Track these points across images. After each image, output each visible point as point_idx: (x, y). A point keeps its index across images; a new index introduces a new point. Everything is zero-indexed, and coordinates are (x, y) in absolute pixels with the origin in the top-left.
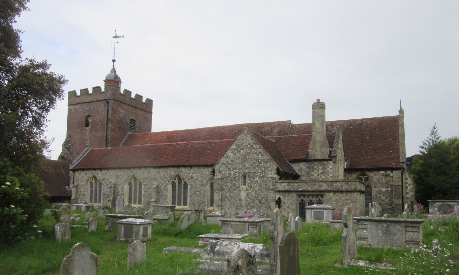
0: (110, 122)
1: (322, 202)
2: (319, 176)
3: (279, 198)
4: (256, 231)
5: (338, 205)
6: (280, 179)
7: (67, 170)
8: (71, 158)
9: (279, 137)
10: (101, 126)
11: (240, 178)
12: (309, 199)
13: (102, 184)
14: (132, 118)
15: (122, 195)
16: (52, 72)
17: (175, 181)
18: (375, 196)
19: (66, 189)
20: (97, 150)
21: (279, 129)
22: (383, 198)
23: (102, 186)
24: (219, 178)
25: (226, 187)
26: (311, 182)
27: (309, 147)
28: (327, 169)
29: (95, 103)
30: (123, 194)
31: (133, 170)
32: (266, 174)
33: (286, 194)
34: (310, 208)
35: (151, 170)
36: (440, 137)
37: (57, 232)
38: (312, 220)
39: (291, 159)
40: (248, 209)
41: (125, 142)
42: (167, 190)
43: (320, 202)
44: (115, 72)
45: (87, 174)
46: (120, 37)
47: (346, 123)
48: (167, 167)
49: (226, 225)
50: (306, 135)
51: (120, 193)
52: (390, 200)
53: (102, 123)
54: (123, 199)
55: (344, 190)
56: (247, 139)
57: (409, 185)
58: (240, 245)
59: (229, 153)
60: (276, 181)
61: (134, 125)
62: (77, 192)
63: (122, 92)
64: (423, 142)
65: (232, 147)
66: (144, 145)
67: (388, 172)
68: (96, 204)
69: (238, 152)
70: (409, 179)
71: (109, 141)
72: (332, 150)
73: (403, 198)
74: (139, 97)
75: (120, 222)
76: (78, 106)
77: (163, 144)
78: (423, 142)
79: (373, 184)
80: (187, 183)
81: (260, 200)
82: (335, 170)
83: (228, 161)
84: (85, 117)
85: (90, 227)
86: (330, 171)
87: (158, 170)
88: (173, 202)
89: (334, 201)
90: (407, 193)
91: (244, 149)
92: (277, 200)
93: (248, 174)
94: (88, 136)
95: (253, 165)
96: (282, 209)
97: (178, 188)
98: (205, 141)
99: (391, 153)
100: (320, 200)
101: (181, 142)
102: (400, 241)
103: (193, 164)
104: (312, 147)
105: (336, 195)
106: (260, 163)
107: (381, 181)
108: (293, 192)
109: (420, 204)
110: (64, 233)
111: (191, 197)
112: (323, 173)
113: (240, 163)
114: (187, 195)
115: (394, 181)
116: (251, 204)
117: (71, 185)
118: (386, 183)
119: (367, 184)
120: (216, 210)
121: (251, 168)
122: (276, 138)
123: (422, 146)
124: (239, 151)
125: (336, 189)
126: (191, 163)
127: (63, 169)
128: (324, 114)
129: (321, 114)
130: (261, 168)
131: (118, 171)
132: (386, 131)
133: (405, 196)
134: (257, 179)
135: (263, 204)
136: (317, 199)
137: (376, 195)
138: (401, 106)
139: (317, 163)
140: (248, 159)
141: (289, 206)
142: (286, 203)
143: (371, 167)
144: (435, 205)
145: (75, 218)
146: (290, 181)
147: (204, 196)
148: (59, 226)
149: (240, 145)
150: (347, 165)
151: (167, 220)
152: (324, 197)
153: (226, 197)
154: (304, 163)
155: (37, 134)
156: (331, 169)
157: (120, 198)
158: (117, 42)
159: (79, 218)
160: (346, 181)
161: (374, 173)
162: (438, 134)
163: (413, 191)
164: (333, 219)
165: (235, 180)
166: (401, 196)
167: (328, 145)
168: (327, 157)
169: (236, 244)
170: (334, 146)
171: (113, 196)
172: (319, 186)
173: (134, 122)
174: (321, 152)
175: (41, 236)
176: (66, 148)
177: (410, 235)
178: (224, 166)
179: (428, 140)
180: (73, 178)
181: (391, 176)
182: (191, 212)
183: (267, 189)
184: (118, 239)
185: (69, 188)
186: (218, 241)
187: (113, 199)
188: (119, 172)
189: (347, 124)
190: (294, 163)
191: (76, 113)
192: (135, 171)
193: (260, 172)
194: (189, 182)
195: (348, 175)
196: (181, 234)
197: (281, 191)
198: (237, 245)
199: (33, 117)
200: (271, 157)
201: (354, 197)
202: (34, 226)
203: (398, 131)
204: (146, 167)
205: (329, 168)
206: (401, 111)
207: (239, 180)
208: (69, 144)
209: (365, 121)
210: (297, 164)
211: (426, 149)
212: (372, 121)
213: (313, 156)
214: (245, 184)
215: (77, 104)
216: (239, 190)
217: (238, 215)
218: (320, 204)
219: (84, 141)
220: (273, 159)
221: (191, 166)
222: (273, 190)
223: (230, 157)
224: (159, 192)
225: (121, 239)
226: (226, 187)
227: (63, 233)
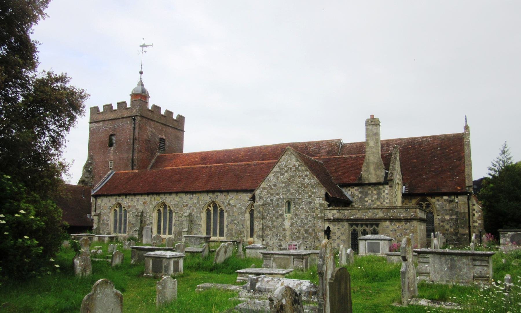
0: (137, 141)
1: (377, 232)
2: (373, 202)
3: (328, 228)
4: (303, 265)
5: (396, 236)
6: (329, 206)
7: (88, 196)
8: (93, 183)
9: (327, 158)
10: (127, 146)
11: (283, 204)
12: (362, 228)
13: (127, 211)
15: (149, 225)
16: (72, 86)
17: (210, 208)
18: (437, 225)
19: (87, 217)
20: (122, 173)
21: (327, 149)
22: (447, 227)
23: (128, 214)
26: (364, 209)
27: (362, 169)
28: (383, 194)
29: (120, 120)
30: (151, 223)
31: (162, 196)
32: (313, 200)
33: (335, 222)
34: (364, 239)
35: (183, 195)
36: (512, 157)
37: (77, 266)
38: (366, 253)
39: (342, 182)
40: (293, 240)
41: (154, 164)
42: (200, 219)
43: (375, 232)
44: (142, 85)
45: (111, 200)
46: (149, 46)
47: (403, 142)
48: (201, 192)
49: (267, 258)
50: (358, 155)
51: (148, 222)
52: (455, 230)
53: (127, 142)
54: (151, 229)
55: (403, 218)
57: (477, 212)
58: (284, 282)
59: (271, 176)
62: (99, 222)
63: (150, 107)
64: (492, 163)
65: (274, 170)
66: (175, 168)
67: (453, 197)
68: (121, 234)
69: (281, 175)
70: (476, 205)
71: (136, 163)
72: (388, 173)
73: (470, 227)
74: (169, 113)
75: (148, 255)
76: (101, 124)
77: (196, 166)
78: (492, 163)
79: (435, 212)
80: (223, 210)
81: (307, 229)
82: (392, 196)
83: (270, 185)
84: (109, 136)
85: (114, 261)
86: (386, 196)
88: (208, 232)
89: (391, 231)
90: (475, 222)
91: (288, 172)
93: (293, 200)
94: (112, 158)
95: (298, 189)
96: (332, 240)
97: (213, 216)
98: (244, 163)
99: (456, 176)
100: (374, 230)
101: (216, 164)
102: (467, 277)
103: (231, 189)
105: (394, 223)
106: (306, 187)
107: (444, 208)
108: (344, 220)
109: (490, 234)
110: (84, 267)
112: (378, 199)
113: (283, 188)
114: (224, 224)
115: (459, 207)
116: (296, 234)
117: (93, 213)
118: (450, 210)
119: (428, 211)
122: (324, 159)
124: (283, 174)
125: (393, 217)
126: (228, 188)
127: (84, 195)
128: (379, 132)
129: (375, 131)
130: (307, 193)
131: (146, 197)
132: (450, 150)
133: (473, 224)
134: (303, 206)
136: (371, 229)
137: (439, 224)
138: (466, 121)
140: (293, 182)
142: (335, 233)
144: (507, 235)
145: (97, 251)
146: (340, 208)
147: (243, 225)
148: (78, 259)
149: (284, 167)
150: (405, 189)
151: (201, 252)
152: (380, 226)
153: (268, 227)
154: (356, 188)
155: (54, 155)
156: (387, 194)
157: (148, 228)
158: (145, 52)
159: (101, 250)
160: (405, 207)
161: (436, 198)
162: (509, 154)
163: (481, 220)
164: (390, 251)
165: (278, 207)
166: (468, 225)
167: (384, 167)
168: (382, 180)
169: (279, 280)
171: (140, 226)
172: (374, 214)
173: (163, 141)
174: (376, 175)
175: (58, 271)
177: (478, 270)
178: (266, 191)
179: (498, 161)
180: (95, 205)
182: (228, 244)
183: (314, 218)
184: (145, 274)
185: (91, 216)
186: (259, 276)
187: (140, 228)
188: (147, 199)
189: (405, 143)
190: (345, 188)
191: (99, 132)
192: (165, 197)
193: (306, 198)
195: (406, 201)
196: (217, 269)
197: (330, 219)
198: (281, 282)
199: (51, 136)
200: (318, 181)
201: (413, 226)
202: (50, 260)
204: (177, 193)
206: (466, 128)
207: (282, 206)
208: (91, 167)
209: (425, 139)
210: (348, 189)
211: (495, 171)
214: (289, 211)
215: (99, 122)
217: (282, 246)
218: (375, 234)
219: (107, 163)
220: (321, 183)
221: (228, 191)
222: (321, 218)
224: (192, 221)
225: (148, 275)
227: (83, 267)
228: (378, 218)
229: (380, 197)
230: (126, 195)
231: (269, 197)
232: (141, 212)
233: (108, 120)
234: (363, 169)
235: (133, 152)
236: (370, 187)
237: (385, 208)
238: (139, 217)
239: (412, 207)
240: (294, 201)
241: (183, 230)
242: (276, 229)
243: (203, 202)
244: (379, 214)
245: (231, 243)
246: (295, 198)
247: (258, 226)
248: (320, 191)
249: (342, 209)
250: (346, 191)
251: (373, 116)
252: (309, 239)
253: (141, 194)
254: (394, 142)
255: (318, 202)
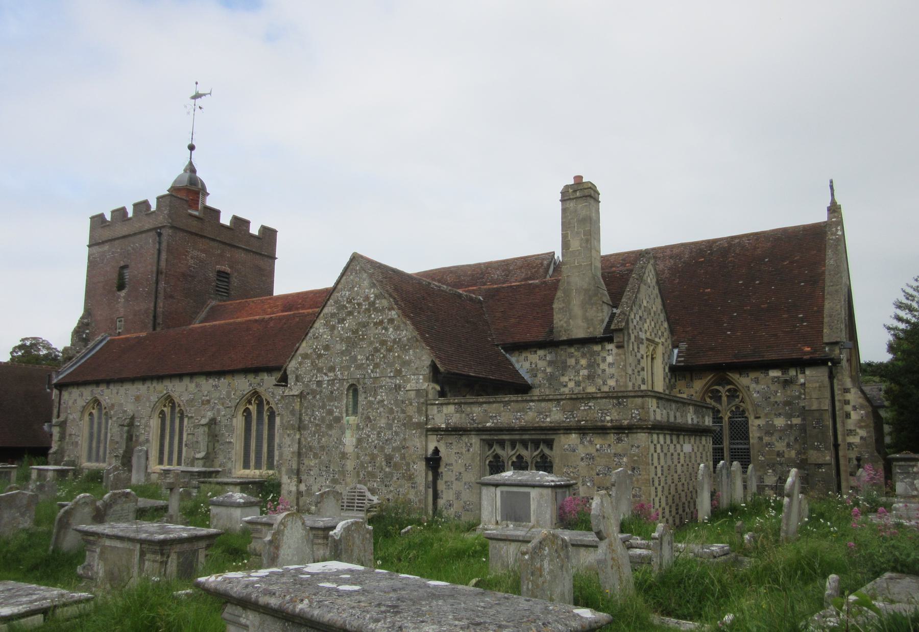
1: (551, 462)
2: (579, 386)
3: (436, 451)
5: (594, 473)
9: (494, 289)
10: (146, 287)
11: (342, 393)
12: (513, 452)
14: (223, 270)
19: (43, 429)
22: (780, 446)
23: (110, 421)
24: (293, 396)
25: (310, 418)
28: (602, 366)
30: (147, 441)
32: (404, 381)
34: (491, 482)
35: (202, 381)
38: (497, 522)
39: (510, 341)
40: (360, 482)
45: (85, 394)
46: (205, 95)
48: (232, 372)
51: (142, 438)
52: (798, 453)
54: (147, 452)
55: (609, 424)
56: (360, 286)
57: (855, 408)
59: (319, 327)
60: (429, 402)
61: (225, 284)
62: (62, 438)
64: (904, 291)
67: (792, 372)
69: (339, 323)
70: (853, 391)
71: (160, 320)
73: (836, 446)
74: (240, 223)
76: (106, 247)
78: (904, 291)
79: (751, 409)
84: (118, 269)
86: (609, 371)
87: (216, 380)
89: (582, 459)
90: (851, 432)
92: (429, 456)
93: (361, 381)
95: (373, 355)
99: (802, 320)
100: (543, 457)
104: (561, 306)
106: (390, 350)
107: (772, 399)
108: (470, 431)
111: (281, 447)
112: (591, 377)
113: (342, 353)
116: (368, 467)
117: (54, 421)
118: (788, 403)
119: (734, 409)
120: (285, 484)
121: (368, 365)
123: (901, 303)
124: (342, 321)
125: (586, 421)
129: (583, 213)
130: (391, 365)
133: (844, 440)
134: (382, 396)
135: (396, 466)
137: (761, 439)
138: (832, 195)
139: (576, 350)
140: (363, 339)
141: (460, 473)
143: (742, 360)
150: (678, 357)
152: (555, 444)
153: (311, 448)
154: (541, 353)
157: (140, 451)
158: (200, 108)
160: (615, 395)
161: (753, 375)
163: (866, 427)
167: (607, 298)
170: (624, 300)
171: (127, 447)
172: (540, 413)
174: (586, 319)
176: (79, 338)
181: (802, 384)
187: (125, 452)
188: (141, 389)
189: (691, 253)
190: (517, 354)
192: (172, 384)
193: (390, 377)
194: (278, 408)
195: (681, 384)
200: (416, 333)
201: (638, 447)
203: (824, 260)
204: (192, 375)
205: (607, 363)
206: (834, 209)
208: (87, 331)
209: (737, 241)
210: (524, 355)
212: (757, 240)
213: (565, 331)
214: (355, 412)
215: (103, 243)
216: (340, 429)
222: (419, 425)
223: (321, 336)
224: (216, 436)
226: (310, 418)
228: (547, 424)
229: (595, 372)
230: (108, 382)
231: (314, 375)
232: (130, 417)
233: (118, 238)
234: (556, 306)
235: (156, 298)
236: (572, 350)
237: (565, 399)
238: (126, 428)
239: (633, 394)
240: (365, 384)
241: (198, 456)
242: (327, 453)
243: (237, 394)
244: (552, 414)
245: (128, 493)
246: (367, 376)
247: (289, 446)
248: (419, 358)
249: (465, 403)
250: (518, 362)
251: (581, 177)
252: (395, 478)
253: (133, 380)
254: (668, 252)
255: (414, 385)
